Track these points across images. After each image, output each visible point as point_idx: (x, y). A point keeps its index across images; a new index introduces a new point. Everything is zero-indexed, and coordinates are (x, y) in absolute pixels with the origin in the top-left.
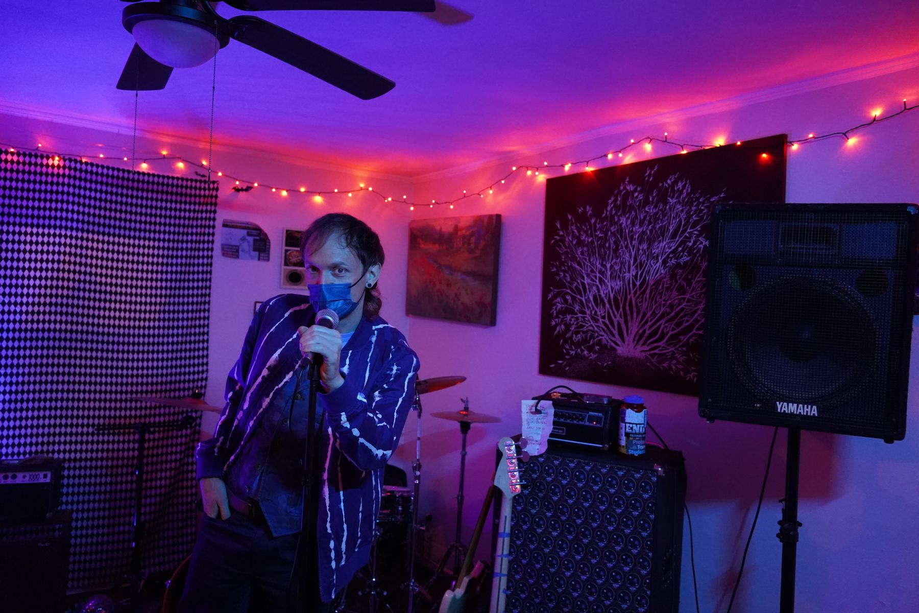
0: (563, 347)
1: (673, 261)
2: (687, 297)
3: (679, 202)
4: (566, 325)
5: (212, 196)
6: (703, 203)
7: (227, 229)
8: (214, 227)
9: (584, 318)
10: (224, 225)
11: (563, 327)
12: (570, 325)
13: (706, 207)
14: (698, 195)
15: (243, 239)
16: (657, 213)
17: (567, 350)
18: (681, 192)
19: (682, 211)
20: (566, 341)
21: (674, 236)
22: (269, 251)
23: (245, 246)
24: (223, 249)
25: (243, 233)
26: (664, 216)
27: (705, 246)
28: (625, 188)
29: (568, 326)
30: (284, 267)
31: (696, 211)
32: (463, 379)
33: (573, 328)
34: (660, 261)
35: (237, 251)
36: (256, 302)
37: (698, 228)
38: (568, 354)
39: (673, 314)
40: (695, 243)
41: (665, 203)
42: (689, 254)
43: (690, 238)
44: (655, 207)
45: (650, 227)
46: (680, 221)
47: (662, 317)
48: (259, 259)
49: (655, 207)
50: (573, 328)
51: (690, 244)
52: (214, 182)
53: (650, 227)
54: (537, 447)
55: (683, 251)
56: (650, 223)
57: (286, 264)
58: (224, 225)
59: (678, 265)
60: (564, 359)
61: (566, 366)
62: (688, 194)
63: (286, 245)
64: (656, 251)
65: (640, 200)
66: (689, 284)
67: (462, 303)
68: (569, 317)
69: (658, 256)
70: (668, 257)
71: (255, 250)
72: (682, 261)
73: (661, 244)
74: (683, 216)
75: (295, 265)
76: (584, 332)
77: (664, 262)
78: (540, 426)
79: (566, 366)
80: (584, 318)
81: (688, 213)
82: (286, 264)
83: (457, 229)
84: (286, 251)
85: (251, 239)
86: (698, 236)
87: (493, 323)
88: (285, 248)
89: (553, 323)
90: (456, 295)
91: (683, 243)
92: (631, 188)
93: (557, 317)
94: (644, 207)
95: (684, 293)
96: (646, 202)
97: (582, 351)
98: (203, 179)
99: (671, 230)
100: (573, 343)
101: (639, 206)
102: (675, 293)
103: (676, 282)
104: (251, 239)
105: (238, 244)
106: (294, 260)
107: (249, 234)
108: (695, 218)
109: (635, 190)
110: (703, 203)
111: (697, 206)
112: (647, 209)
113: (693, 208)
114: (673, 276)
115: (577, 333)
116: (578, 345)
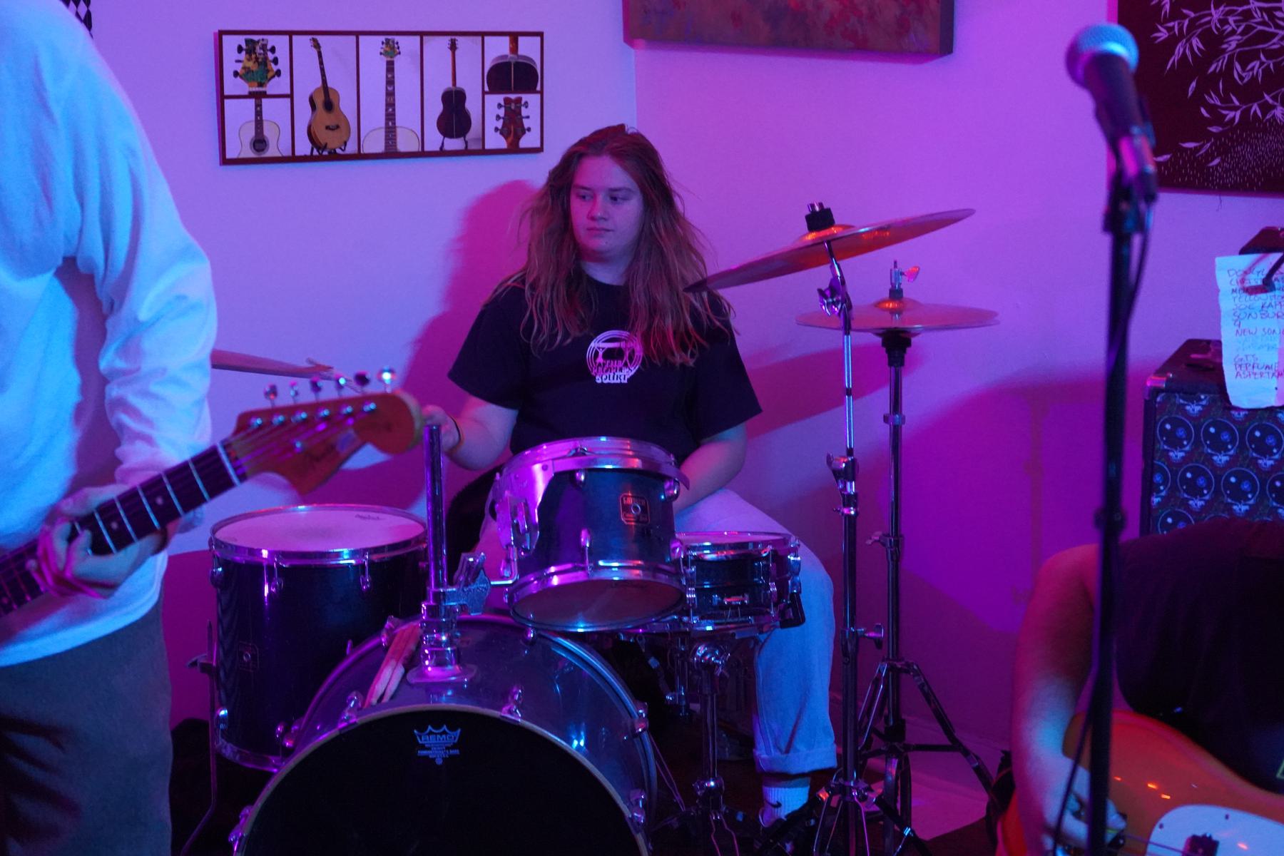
0: (1199, 99)
4: (1207, 37)
9: (1270, 12)
11: (1196, 42)
12: (1223, 37)
17: (1212, 109)
20: (1208, 83)
29: (1214, 42)
32: (968, 213)
33: (1232, 44)
36: (221, 33)
38: (1218, 119)
50: (1232, 44)
54: (1274, 382)
60: (1203, 135)
61: (1209, 156)
68: (1216, 14)
76: (1270, 54)
78: (1272, 323)
79: (1209, 156)
80: (1270, 12)
87: (945, 46)
89: (1163, 34)
93: (1176, 14)
97: (1266, 108)
100: (1231, 86)
115: (1245, 59)
116: (1250, 92)
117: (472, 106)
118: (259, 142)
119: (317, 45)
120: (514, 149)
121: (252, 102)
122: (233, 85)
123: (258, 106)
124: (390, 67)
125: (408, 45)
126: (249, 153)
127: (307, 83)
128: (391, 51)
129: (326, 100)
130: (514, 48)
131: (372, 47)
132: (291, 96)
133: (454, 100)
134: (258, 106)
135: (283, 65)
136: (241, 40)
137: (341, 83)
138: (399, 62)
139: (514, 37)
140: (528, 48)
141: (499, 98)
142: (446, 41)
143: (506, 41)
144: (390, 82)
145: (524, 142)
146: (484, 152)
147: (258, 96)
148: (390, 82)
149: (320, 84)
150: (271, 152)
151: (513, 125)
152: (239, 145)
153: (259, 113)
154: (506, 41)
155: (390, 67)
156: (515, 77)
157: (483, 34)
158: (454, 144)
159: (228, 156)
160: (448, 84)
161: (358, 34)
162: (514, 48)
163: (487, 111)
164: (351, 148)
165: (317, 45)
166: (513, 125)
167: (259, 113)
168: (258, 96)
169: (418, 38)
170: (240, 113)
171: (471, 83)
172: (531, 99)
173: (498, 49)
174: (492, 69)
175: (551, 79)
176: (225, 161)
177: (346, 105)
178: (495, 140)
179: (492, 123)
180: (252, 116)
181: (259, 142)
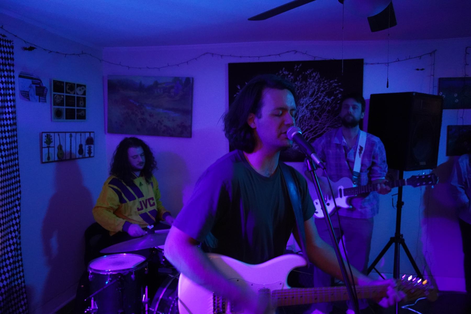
1: (312, 107)
2: (319, 122)
3: (314, 82)
5: (10, 53)
6: (326, 83)
7: (21, 79)
8: (14, 77)
10: (20, 76)
13: (328, 85)
14: (324, 79)
15: (30, 87)
16: (302, 85)
18: (315, 77)
19: (316, 85)
21: (311, 96)
22: (46, 95)
23: (32, 92)
24: (22, 94)
25: (30, 81)
26: (306, 87)
27: (328, 101)
28: (282, 73)
30: (53, 107)
31: (323, 86)
34: (305, 106)
35: (28, 96)
36: (43, 133)
37: (324, 93)
39: (312, 129)
40: (323, 99)
41: (307, 81)
42: (320, 104)
43: (320, 97)
44: (301, 82)
45: (298, 91)
46: (315, 89)
47: (306, 130)
48: (39, 101)
49: (301, 82)
51: (320, 100)
52: (10, 42)
53: (298, 91)
55: (317, 102)
56: (298, 89)
57: (54, 105)
58: (20, 76)
59: (314, 109)
62: (318, 78)
63: (54, 91)
64: (302, 102)
65: (292, 79)
66: (320, 116)
67: (165, 126)
69: (303, 104)
70: (309, 105)
71: (37, 95)
72: (316, 107)
73: (305, 99)
74: (316, 88)
75: (58, 105)
77: (307, 107)
81: (319, 86)
82: (54, 105)
83: (156, 84)
84: (54, 95)
85: (34, 86)
86: (324, 97)
88: (53, 93)
90: (159, 121)
91: (317, 99)
92: (286, 73)
94: (294, 82)
95: (318, 120)
96: (295, 80)
98: (4, 38)
99: (310, 93)
101: (291, 81)
102: (313, 120)
103: (314, 115)
104: (34, 86)
105: (28, 90)
106: (58, 101)
107: (33, 83)
108: (322, 89)
109: (289, 74)
110: (326, 83)
111: (324, 84)
112: (296, 83)
113: (322, 85)
114: (312, 113)
117: (83, 147)
118: (49, 158)
119: (59, 135)
120: (90, 157)
121: (47, 149)
122: (44, 145)
123: (49, 149)
124: (71, 139)
125: (74, 135)
126: (47, 161)
127: (57, 144)
128: (71, 136)
129: (60, 147)
130: (90, 135)
131: (68, 135)
132: (54, 147)
133: (81, 146)
134: (49, 149)
135: (53, 140)
136: (46, 134)
137: (63, 144)
138: (73, 139)
139: (90, 132)
140: (92, 135)
141: (87, 146)
142: (79, 134)
143: (89, 134)
144: (71, 143)
145: (92, 155)
146: (85, 158)
147: (48, 147)
148: (71, 143)
149: (58, 144)
150: (51, 160)
151: (90, 152)
152: (45, 159)
153: (49, 151)
154: (89, 134)
155: (71, 139)
156: (90, 141)
157: (85, 132)
158: (81, 156)
159: (43, 161)
160: (79, 143)
161: (66, 132)
162: (90, 135)
163: (86, 148)
164: (64, 158)
165: (59, 135)
166: (90, 152)
167: (49, 151)
168: (48, 147)
169: (75, 133)
170: (45, 151)
171: (84, 143)
172: (92, 146)
173: (87, 135)
174: (87, 140)
175: (95, 142)
176: (43, 163)
177: (63, 149)
178: (87, 155)
179: (87, 151)
180: (47, 152)
181: (49, 158)
